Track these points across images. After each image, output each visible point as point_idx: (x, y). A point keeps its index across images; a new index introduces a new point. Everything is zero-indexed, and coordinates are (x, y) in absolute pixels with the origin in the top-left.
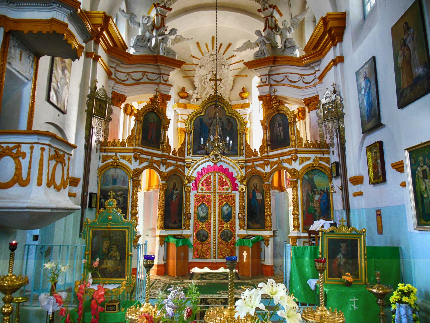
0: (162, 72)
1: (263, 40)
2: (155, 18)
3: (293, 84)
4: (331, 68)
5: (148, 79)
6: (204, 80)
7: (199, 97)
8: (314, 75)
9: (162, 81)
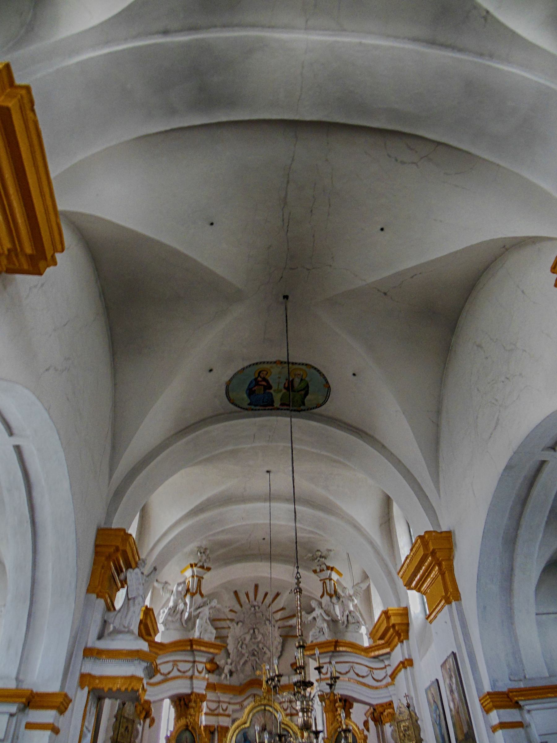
0: (197, 659)
1: (321, 614)
2: (191, 579)
3: (361, 679)
4: (400, 670)
5: (179, 670)
6: (240, 643)
7: (234, 669)
8: (384, 670)
9: (196, 673)
